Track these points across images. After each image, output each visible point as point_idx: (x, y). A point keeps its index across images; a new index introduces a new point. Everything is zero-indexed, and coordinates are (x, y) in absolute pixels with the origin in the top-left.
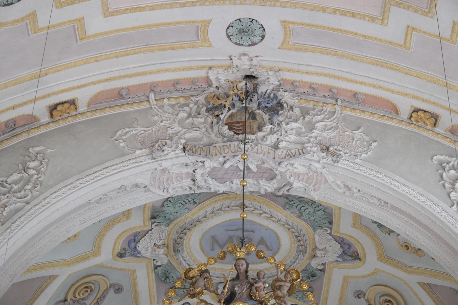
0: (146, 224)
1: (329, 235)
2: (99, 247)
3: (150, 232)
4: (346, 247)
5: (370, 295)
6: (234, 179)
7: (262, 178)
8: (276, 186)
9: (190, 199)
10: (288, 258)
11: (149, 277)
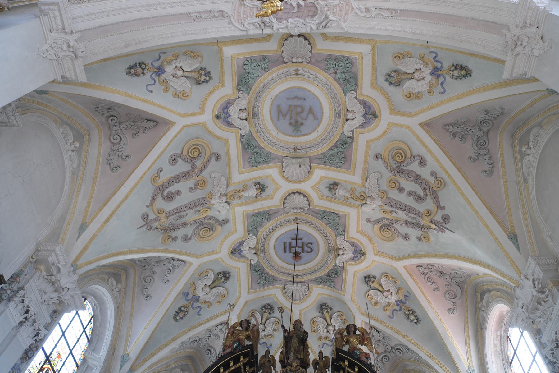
0: (234, 92)
1: (355, 99)
2: (203, 108)
3: (237, 100)
4: (367, 109)
5: (385, 155)
6: (289, 18)
7: (307, 16)
8: (317, 22)
9: (262, 64)
10: (328, 127)
11: (237, 147)
